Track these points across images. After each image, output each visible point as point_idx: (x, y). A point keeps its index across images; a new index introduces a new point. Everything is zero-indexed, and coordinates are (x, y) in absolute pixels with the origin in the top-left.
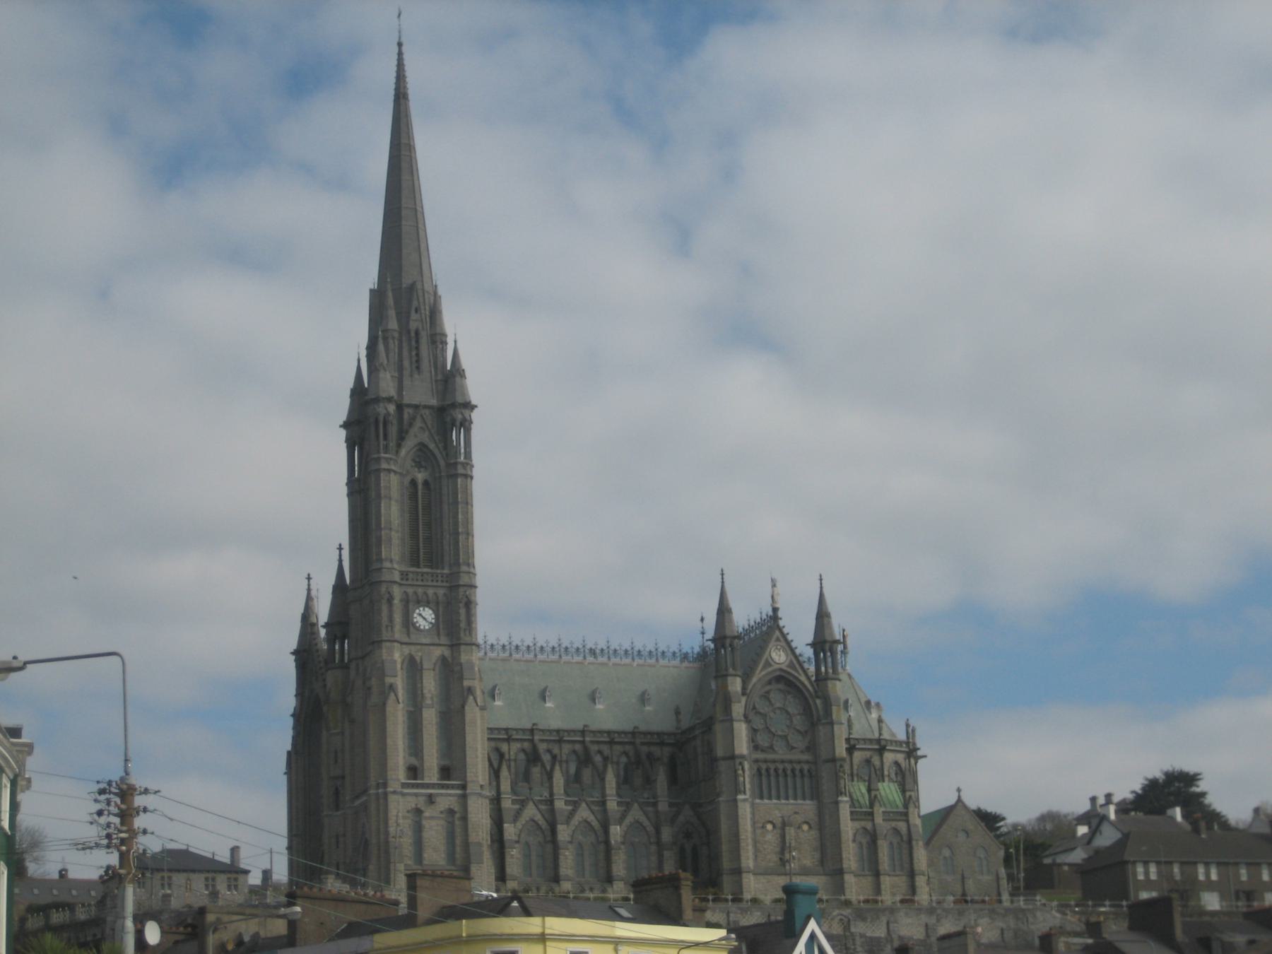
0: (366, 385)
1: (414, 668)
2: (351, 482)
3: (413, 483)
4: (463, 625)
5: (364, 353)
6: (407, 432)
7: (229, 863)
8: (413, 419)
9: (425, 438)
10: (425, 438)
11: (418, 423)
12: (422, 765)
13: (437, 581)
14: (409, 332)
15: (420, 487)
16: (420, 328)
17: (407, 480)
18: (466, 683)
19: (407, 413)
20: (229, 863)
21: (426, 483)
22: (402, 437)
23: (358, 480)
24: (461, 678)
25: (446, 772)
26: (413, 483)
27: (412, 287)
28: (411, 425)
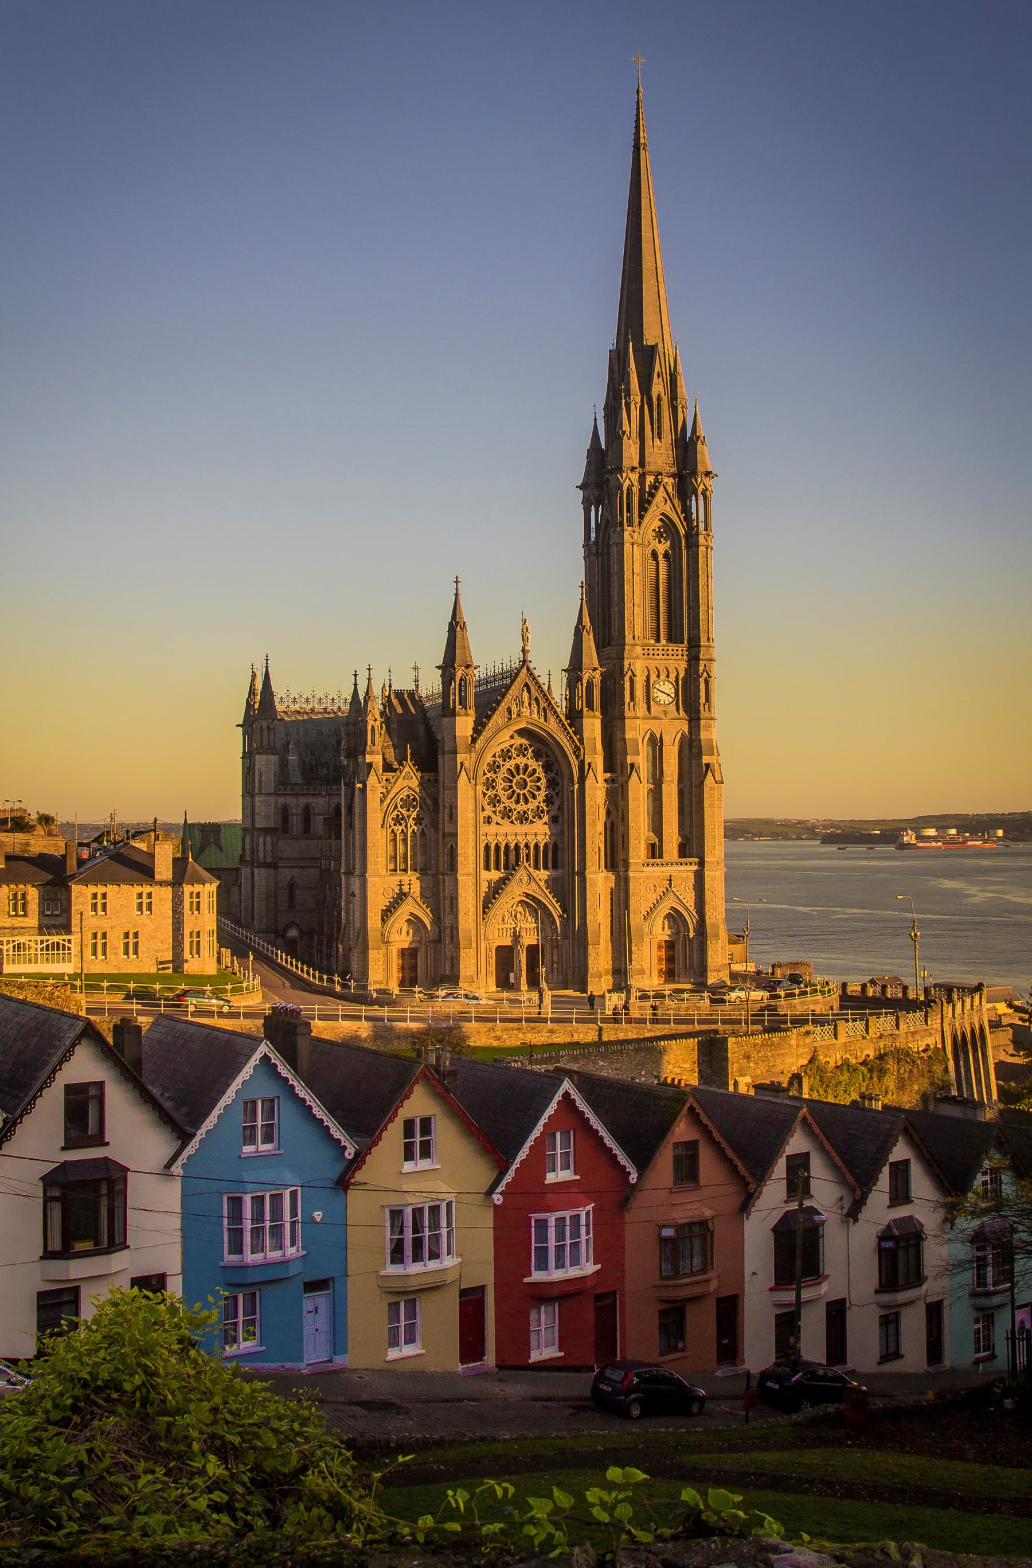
0: (603, 447)
1: (656, 743)
2: (587, 545)
3: (654, 555)
4: (702, 700)
5: (600, 416)
6: (649, 503)
7: (547, 1182)
8: (655, 487)
9: (667, 509)
10: (667, 509)
11: (661, 494)
12: (661, 841)
13: (677, 655)
14: (650, 398)
15: (660, 558)
16: (663, 393)
17: (648, 552)
18: (706, 759)
19: (650, 479)
20: (547, 1182)
21: (666, 555)
22: (645, 504)
23: (596, 543)
24: (700, 755)
25: (684, 851)
26: (654, 555)
27: (653, 349)
28: (653, 496)
